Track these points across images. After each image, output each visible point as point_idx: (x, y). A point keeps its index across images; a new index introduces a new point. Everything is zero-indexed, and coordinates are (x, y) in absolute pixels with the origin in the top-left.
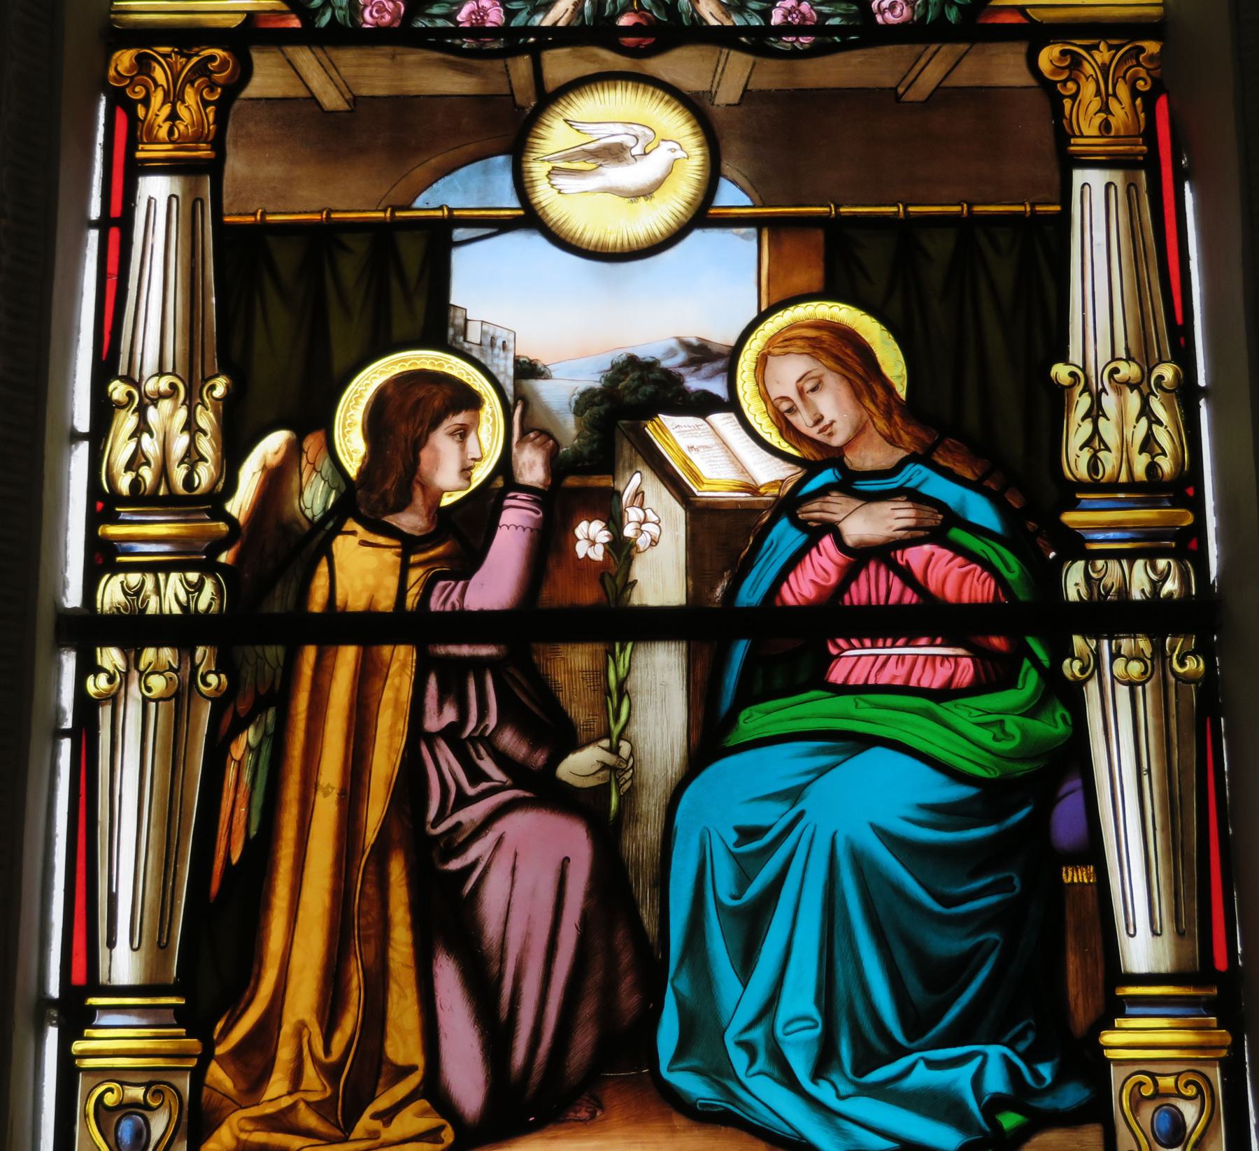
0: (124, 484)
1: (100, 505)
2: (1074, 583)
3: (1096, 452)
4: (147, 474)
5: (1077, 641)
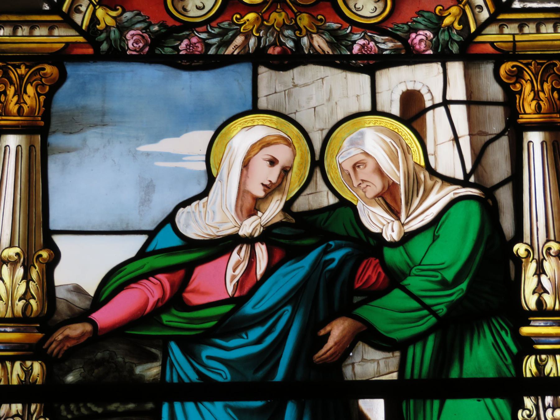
3: (540, 295)
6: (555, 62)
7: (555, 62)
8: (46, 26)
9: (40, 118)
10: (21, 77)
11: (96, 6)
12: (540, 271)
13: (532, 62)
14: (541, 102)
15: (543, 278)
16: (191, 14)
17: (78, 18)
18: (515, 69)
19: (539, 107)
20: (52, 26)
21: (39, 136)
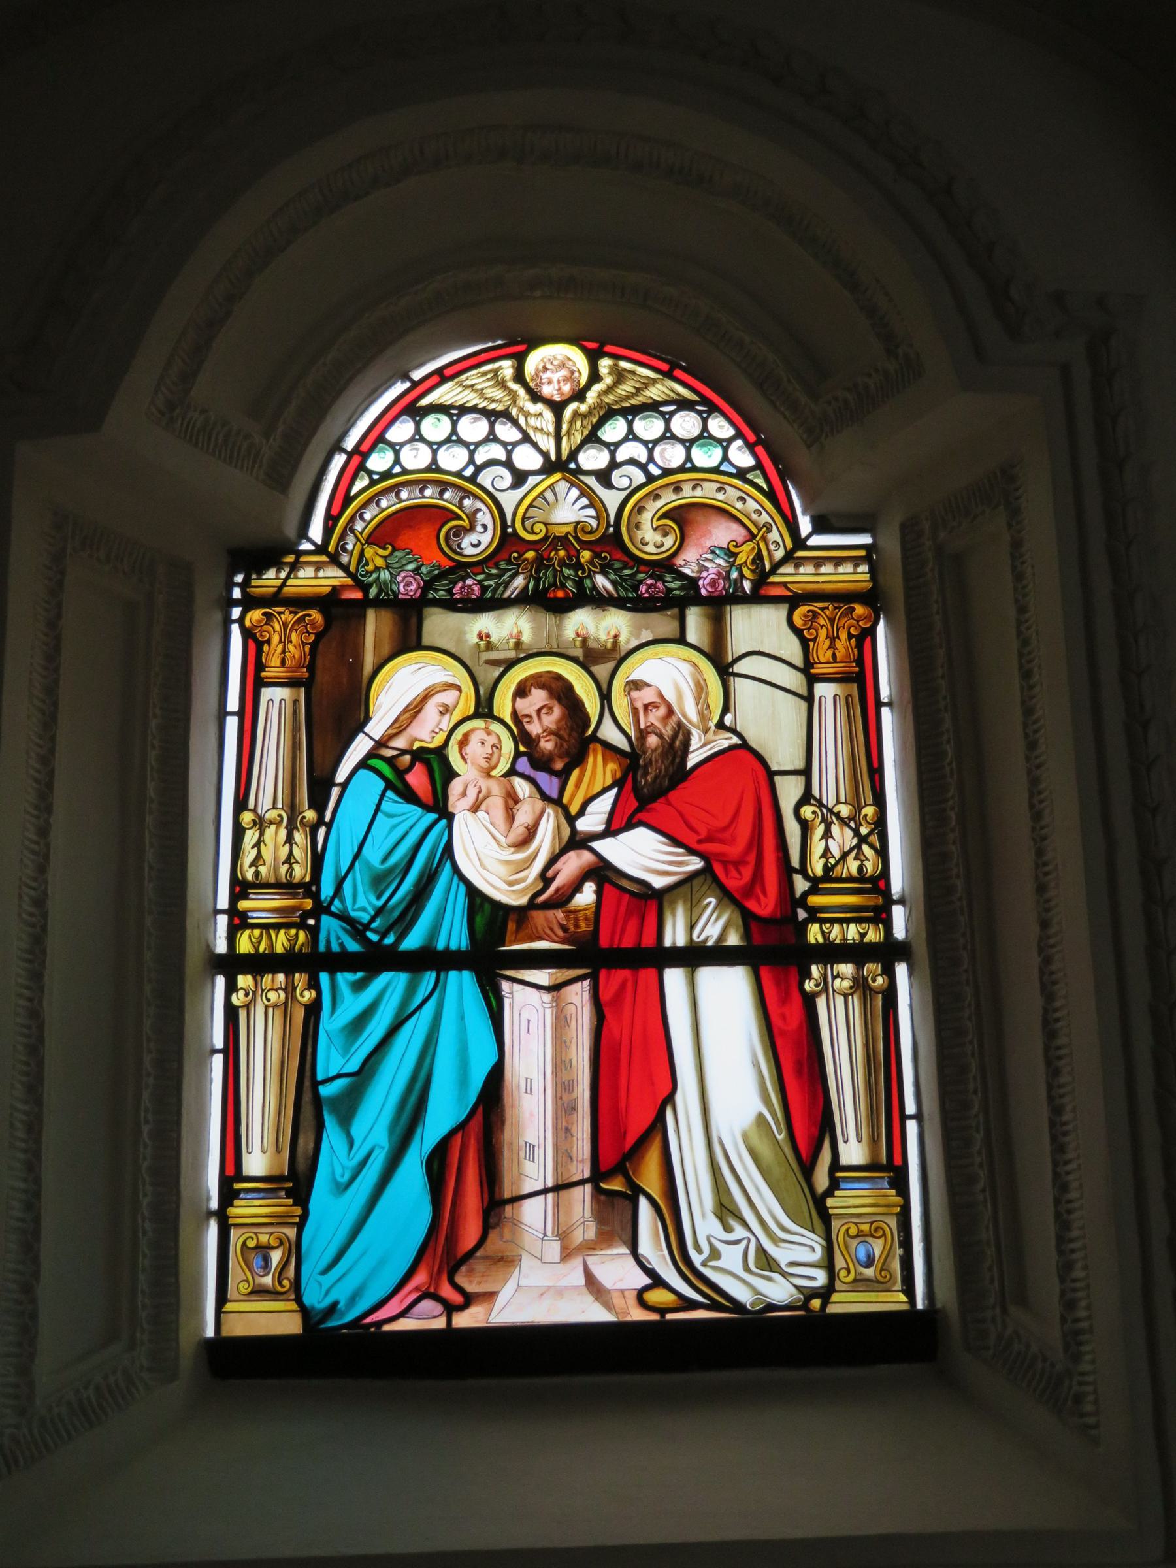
0: (249, 875)
1: (238, 889)
2: (814, 934)
4: (263, 870)
5: (814, 968)
6: (852, 605)
7: (852, 605)
8: (312, 566)
9: (305, 670)
10: (285, 625)
11: (364, 544)
12: (827, 835)
13: (829, 605)
14: (836, 651)
15: (830, 841)
16: (466, 552)
17: (345, 559)
18: (811, 614)
19: (834, 655)
20: (318, 566)
21: (304, 689)
